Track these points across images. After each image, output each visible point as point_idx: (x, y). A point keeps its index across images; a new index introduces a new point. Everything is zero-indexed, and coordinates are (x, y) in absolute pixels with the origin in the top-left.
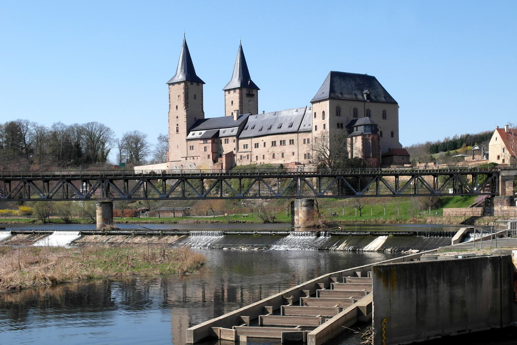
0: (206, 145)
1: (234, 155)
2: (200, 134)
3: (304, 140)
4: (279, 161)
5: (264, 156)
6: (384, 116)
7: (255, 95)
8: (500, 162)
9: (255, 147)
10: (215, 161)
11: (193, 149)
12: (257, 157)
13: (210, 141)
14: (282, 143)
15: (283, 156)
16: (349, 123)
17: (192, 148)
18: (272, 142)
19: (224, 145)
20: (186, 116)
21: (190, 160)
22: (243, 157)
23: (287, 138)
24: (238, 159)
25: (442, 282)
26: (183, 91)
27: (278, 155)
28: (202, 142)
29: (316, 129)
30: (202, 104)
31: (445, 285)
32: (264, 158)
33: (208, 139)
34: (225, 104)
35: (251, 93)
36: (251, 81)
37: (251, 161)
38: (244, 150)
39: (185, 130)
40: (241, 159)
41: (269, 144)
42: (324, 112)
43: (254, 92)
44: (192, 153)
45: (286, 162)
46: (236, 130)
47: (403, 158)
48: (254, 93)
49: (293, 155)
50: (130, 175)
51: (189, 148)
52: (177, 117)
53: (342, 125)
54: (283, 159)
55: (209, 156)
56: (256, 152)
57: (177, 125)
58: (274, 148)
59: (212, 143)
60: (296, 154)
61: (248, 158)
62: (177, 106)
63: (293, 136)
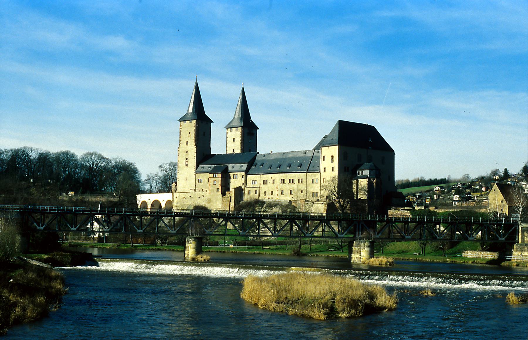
0: (215, 179)
1: (243, 190)
4: (286, 198)
5: (272, 192)
9: (264, 184)
10: (223, 194)
12: (265, 192)
13: (220, 175)
14: (292, 181)
17: (200, 181)
19: (232, 181)
20: (196, 152)
26: (194, 128)
28: (211, 175)
32: (272, 194)
34: (227, 141)
36: (251, 120)
37: (259, 195)
39: (194, 164)
41: (278, 182)
42: (332, 156)
46: (245, 166)
51: (197, 181)
52: (187, 152)
54: (292, 196)
55: (218, 189)
56: (264, 188)
59: (221, 178)
62: (187, 142)
63: (302, 175)
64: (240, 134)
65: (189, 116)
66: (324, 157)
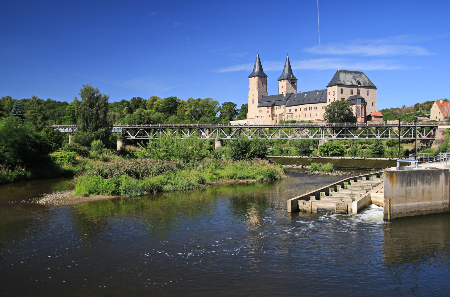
0: (268, 110)
3: (323, 107)
4: (307, 119)
6: (368, 94)
8: (437, 120)
11: (261, 112)
13: (270, 108)
14: (310, 109)
15: (310, 116)
16: (348, 98)
17: (261, 111)
18: (305, 108)
23: (313, 106)
25: (419, 181)
27: (308, 115)
29: (330, 101)
31: (421, 182)
32: (300, 117)
33: (269, 107)
35: (293, 82)
36: (293, 75)
38: (289, 113)
40: (287, 117)
43: (294, 81)
44: (260, 114)
45: (312, 119)
50: (252, 126)
52: (253, 95)
53: (344, 98)
54: (311, 118)
55: (270, 116)
56: (295, 113)
57: (253, 99)
58: (306, 111)
60: (318, 115)
61: (291, 117)
65: (255, 74)
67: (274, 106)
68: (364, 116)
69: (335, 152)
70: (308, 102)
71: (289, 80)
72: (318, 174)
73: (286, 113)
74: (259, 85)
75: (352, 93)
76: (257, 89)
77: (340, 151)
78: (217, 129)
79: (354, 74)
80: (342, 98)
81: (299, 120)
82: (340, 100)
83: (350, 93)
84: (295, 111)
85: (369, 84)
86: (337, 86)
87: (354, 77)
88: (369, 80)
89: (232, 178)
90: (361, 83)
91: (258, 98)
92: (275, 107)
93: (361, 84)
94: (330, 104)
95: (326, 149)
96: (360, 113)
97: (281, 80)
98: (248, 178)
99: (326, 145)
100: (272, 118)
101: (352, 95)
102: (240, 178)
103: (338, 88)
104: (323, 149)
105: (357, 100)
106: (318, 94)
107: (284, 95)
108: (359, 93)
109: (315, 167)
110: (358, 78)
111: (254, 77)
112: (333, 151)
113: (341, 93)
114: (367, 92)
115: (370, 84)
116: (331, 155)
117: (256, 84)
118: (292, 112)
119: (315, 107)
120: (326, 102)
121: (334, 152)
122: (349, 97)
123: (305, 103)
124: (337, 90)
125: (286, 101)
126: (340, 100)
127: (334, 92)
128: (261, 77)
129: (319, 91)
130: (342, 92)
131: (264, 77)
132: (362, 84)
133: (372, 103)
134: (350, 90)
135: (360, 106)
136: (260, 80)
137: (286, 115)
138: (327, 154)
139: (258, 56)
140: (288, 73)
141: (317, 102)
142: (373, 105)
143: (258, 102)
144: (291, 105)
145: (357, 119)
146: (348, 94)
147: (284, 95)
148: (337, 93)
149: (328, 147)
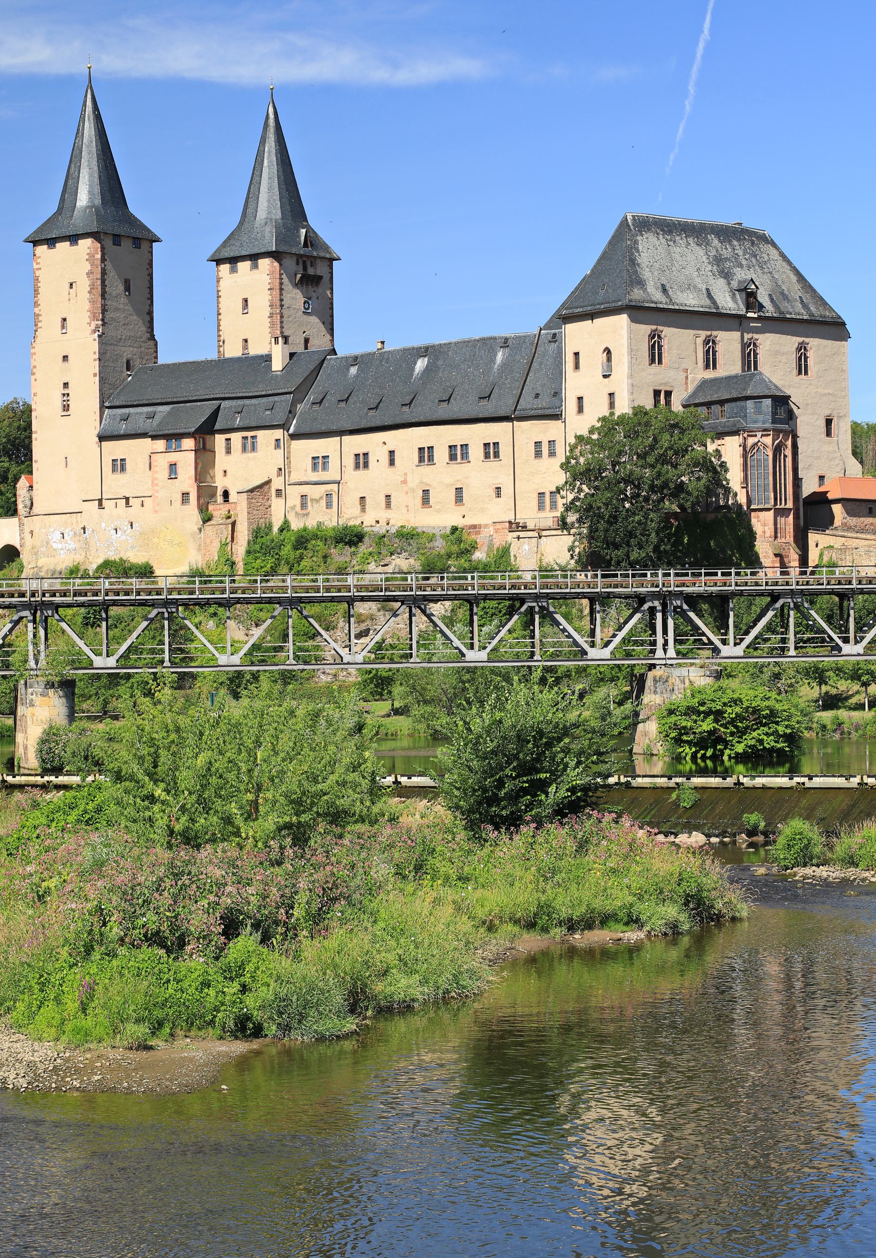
0: (173, 457)
2: (151, 416)
3: (538, 444)
5: (388, 497)
6: (802, 368)
7: (326, 278)
11: (123, 469)
13: (188, 443)
14: (459, 453)
16: (691, 388)
17: (120, 466)
18: (421, 450)
20: (97, 356)
21: (115, 512)
22: (312, 500)
24: (293, 508)
26: (88, 267)
27: (442, 496)
28: (161, 444)
29: (580, 410)
30: (150, 313)
32: (388, 505)
33: (179, 436)
34: (219, 309)
35: (311, 271)
36: (309, 229)
40: (304, 505)
41: (407, 457)
43: (320, 269)
44: (117, 484)
45: (469, 521)
47: (870, 509)
48: (319, 273)
49: (499, 495)
51: (107, 468)
52: (65, 358)
53: (668, 394)
54: (462, 510)
55: (185, 496)
57: (66, 385)
58: (426, 469)
60: (507, 491)
64: (267, 279)
66: (577, 354)
67: (213, 432)
68: (790, 505)
69: (761, 742)
70: (443, 412)
71: (290, 262)
72: (845, 883)
73: (295, 477)
74: (103, 295)
75: (710, 361)
76: (94, 317)
77: (785, 735)
78: (26, 613)
79: (716, 242)
80: (657, 393)
81: (383, 522)
82: (648, 403)
83: (701, 363)
84: (357, 466)
85: (805, 306)
86: (624, 318)
87: (718, 260)
88: (801, 278)
89: (531, 925)
90: (763, 297)
91: (103, 381)
92: (220, 440)
93: (761, 307)
94: (591, 431)
95: (707, 725)
96: (766, 486)
97: (233, 261)
98: (606, 919)
99: (702, 704)
100: (203, 509)
101: (710, 375)
102: (571, 926)
103: (630, 331)
104: (689, 724)
105: (750, 404)
106: (504, 365)
107: (277, 365)
108: (749, 358)
109: (807, 847)
110: (741, 266)
111: (74, 239)
112: (750, 739)
113: (652, 361)
114: (793, 357)
115: (813, 308)
116: (739, 758)
117: (84, 285)
118: (332, 473)
119: (486, 445)
120: (557, 417)
121: (753, 742)
122: (696, 383)
123: (422, 419)
124: (625, 341)
125: (294, 404)
126: (648, 403)
127: (608, 351)
128: (117, 239)
129: (506, 343)
130: (655, 355)
131: (137, 242)
132: (770, 309)
133: (823, 423)
134: (700, 341)
135: (768, 440)
136: (109, 266)
137: (294, 495)
138: (709, 753)
139: (89, 96)
140: (278, 214)
141: (502, 413)
142: (829, 434)
143: (102, 408)
144: (324, 428)
145: (754, 521)
146: (688, 364)
147: (277, 365)
148: (625, 359)
149: (718, 715)
